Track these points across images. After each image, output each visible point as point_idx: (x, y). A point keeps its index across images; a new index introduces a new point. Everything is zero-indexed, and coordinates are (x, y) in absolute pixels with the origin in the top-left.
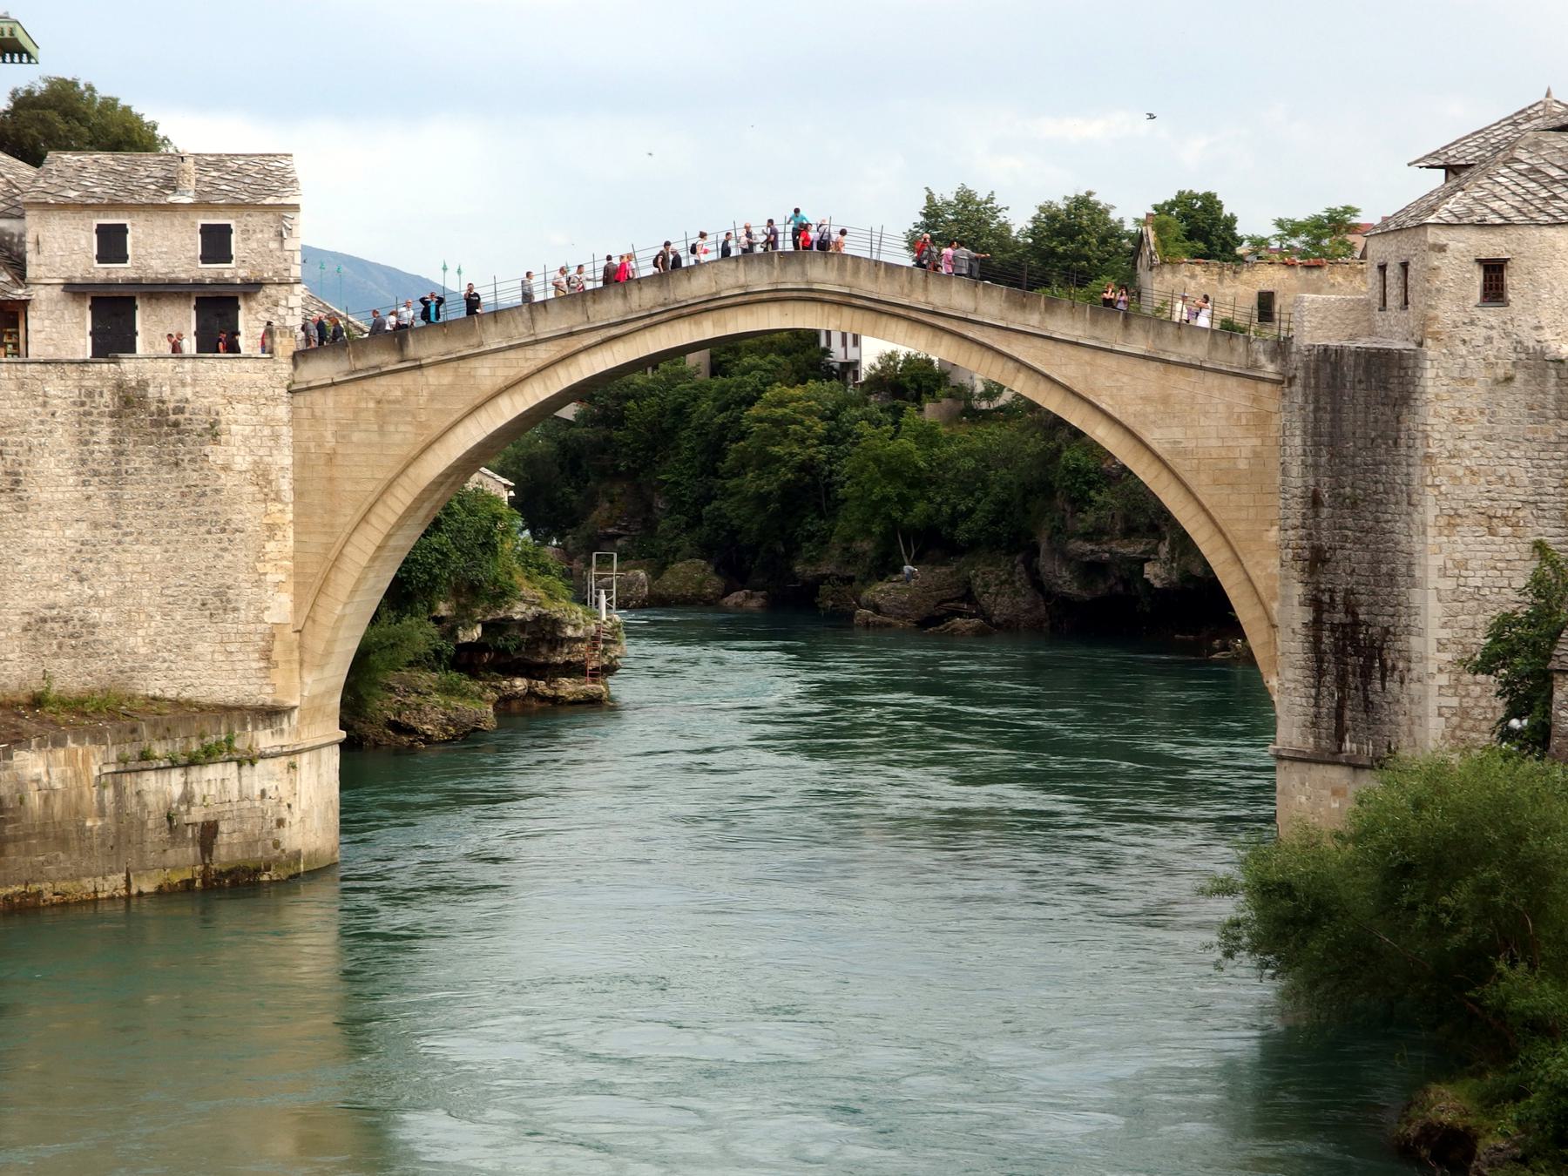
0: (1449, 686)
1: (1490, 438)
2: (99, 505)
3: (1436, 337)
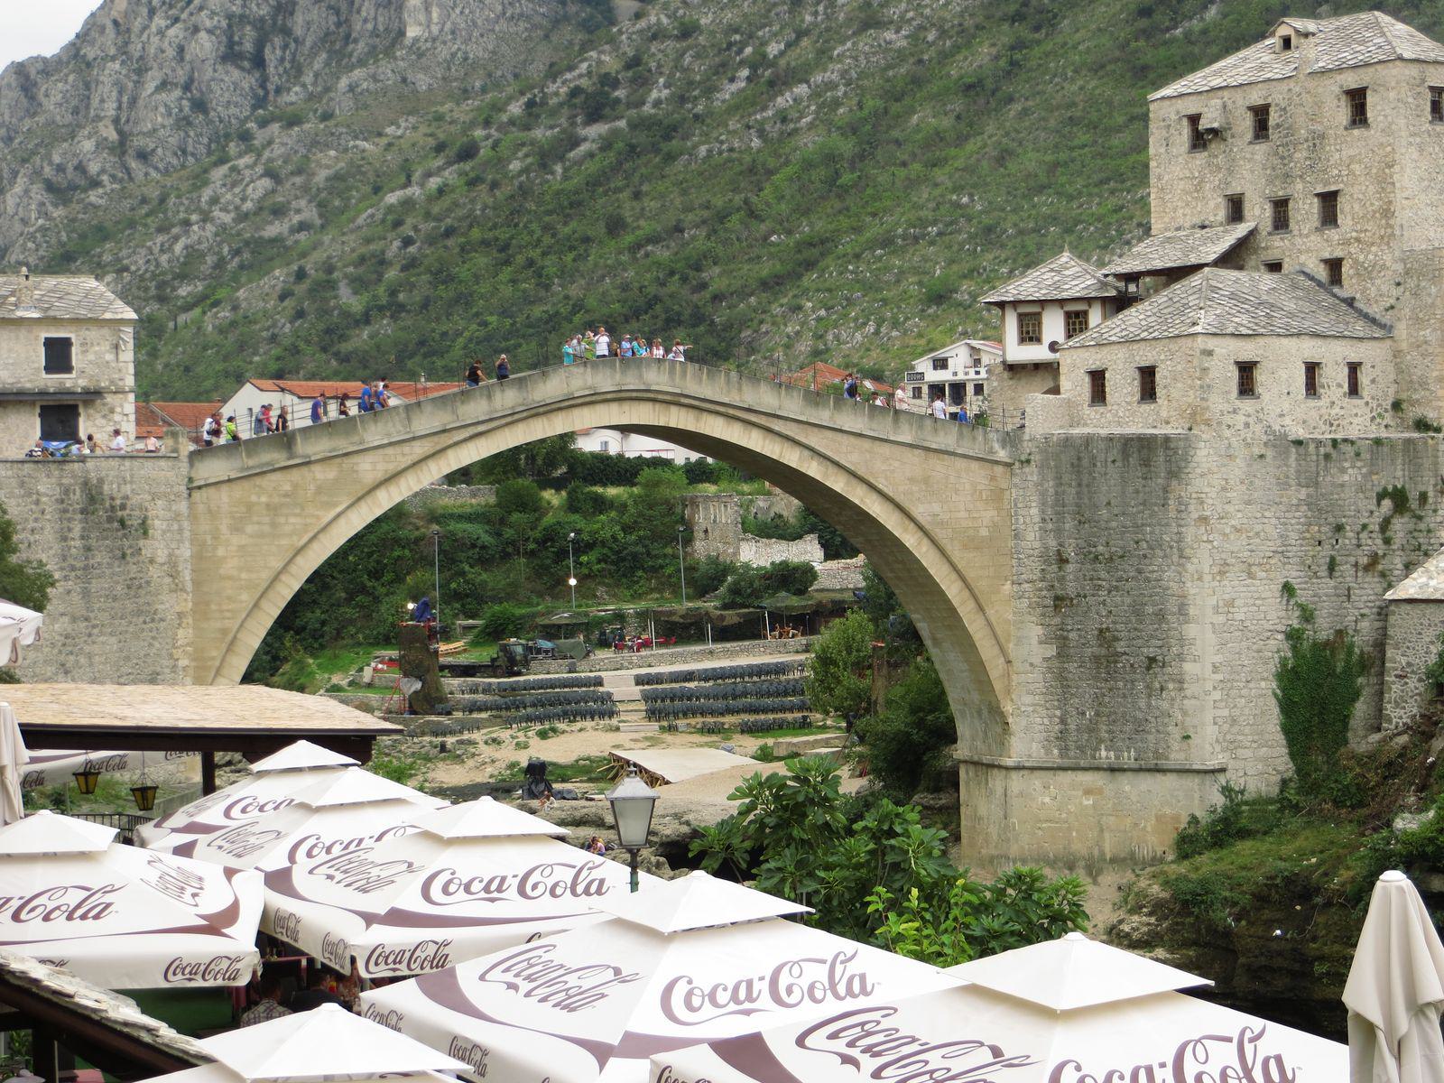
0: (1221, 700)
1: (1248, 503)
2: (76, 598)
3: (1208, 423)
